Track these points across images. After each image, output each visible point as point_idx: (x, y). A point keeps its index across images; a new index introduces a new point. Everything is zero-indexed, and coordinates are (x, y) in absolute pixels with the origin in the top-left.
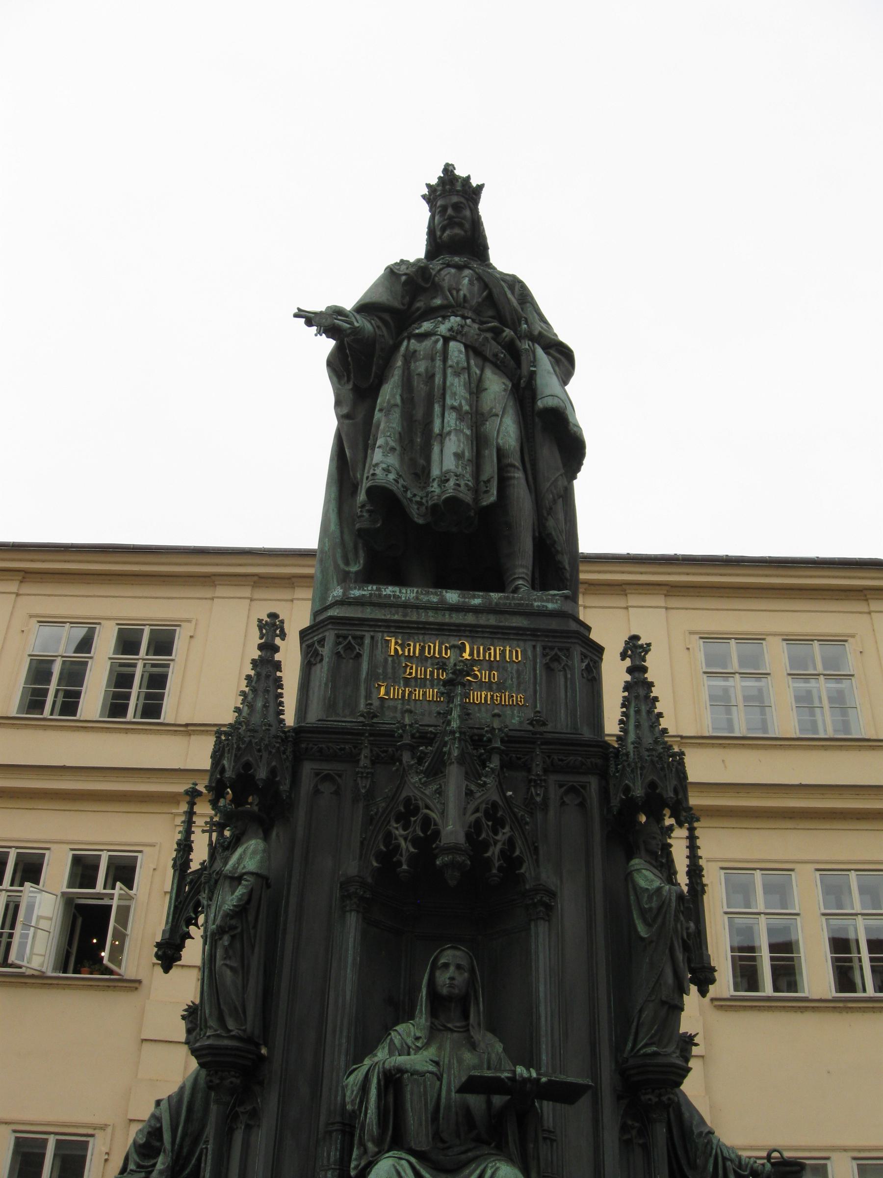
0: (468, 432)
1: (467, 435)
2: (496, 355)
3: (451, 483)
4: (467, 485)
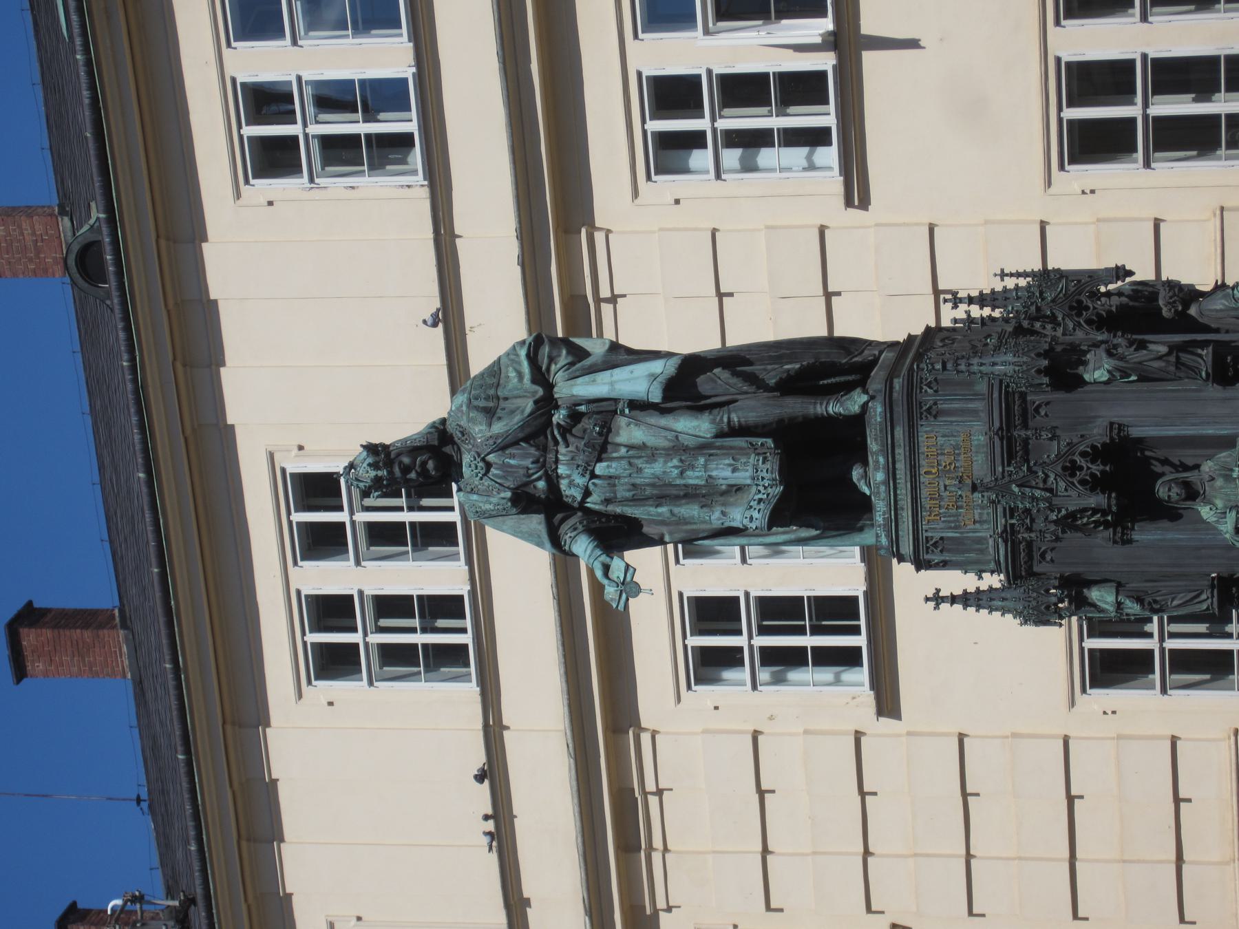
0: (702, 460)
2: (600, 434)
4: (764, 463)
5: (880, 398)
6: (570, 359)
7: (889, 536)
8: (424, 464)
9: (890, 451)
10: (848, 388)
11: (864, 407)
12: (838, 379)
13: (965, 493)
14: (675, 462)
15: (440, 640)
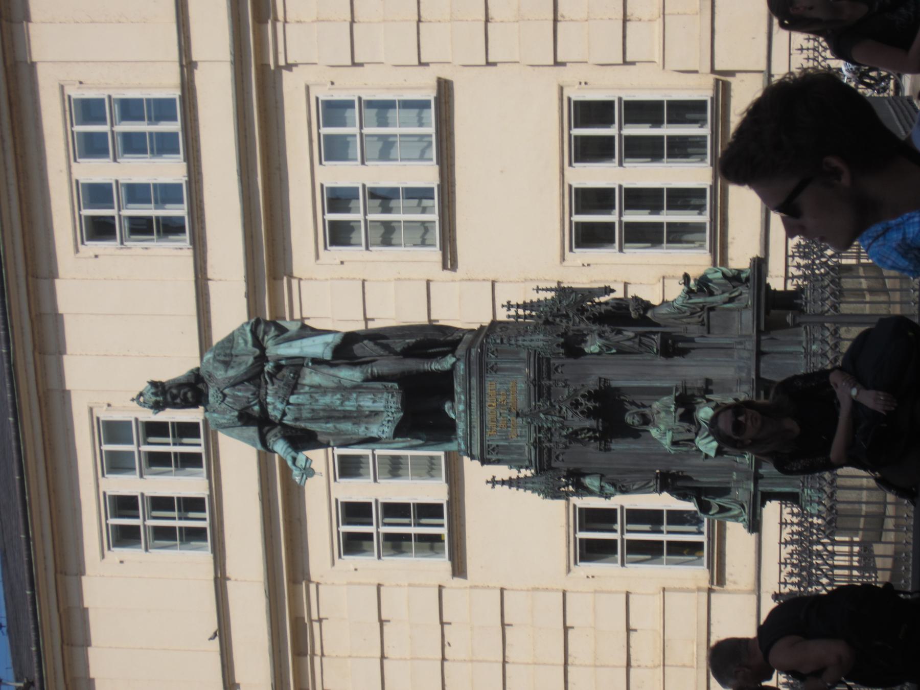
0: (354, 395)
1: (357, 396)
2: (293, 378)
3: (392, 405)
5: (463, 360)
6: (276, 333)
7: (466, 444)
8: (185, 394)
9: (468, 392)
10: (444, 355)
11: (454, 365)
12: (438, 350)
13: (513, 418)
14: (338, 396)
15: (190, 524)
